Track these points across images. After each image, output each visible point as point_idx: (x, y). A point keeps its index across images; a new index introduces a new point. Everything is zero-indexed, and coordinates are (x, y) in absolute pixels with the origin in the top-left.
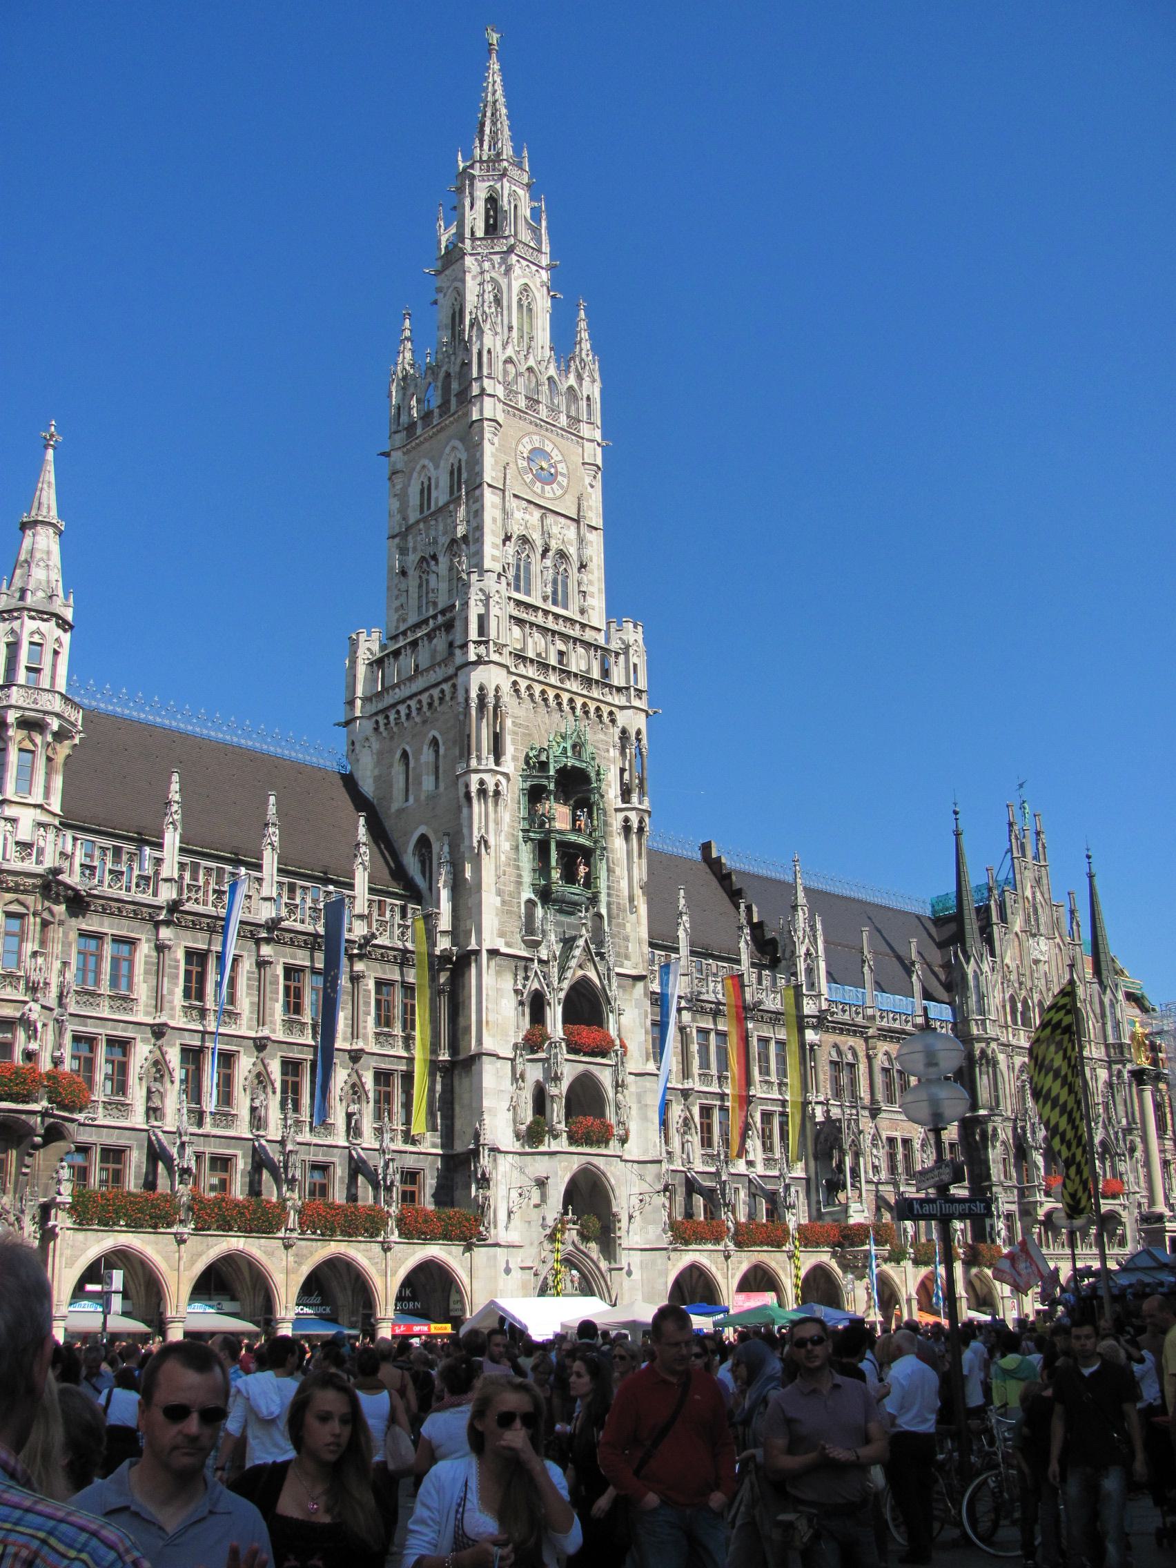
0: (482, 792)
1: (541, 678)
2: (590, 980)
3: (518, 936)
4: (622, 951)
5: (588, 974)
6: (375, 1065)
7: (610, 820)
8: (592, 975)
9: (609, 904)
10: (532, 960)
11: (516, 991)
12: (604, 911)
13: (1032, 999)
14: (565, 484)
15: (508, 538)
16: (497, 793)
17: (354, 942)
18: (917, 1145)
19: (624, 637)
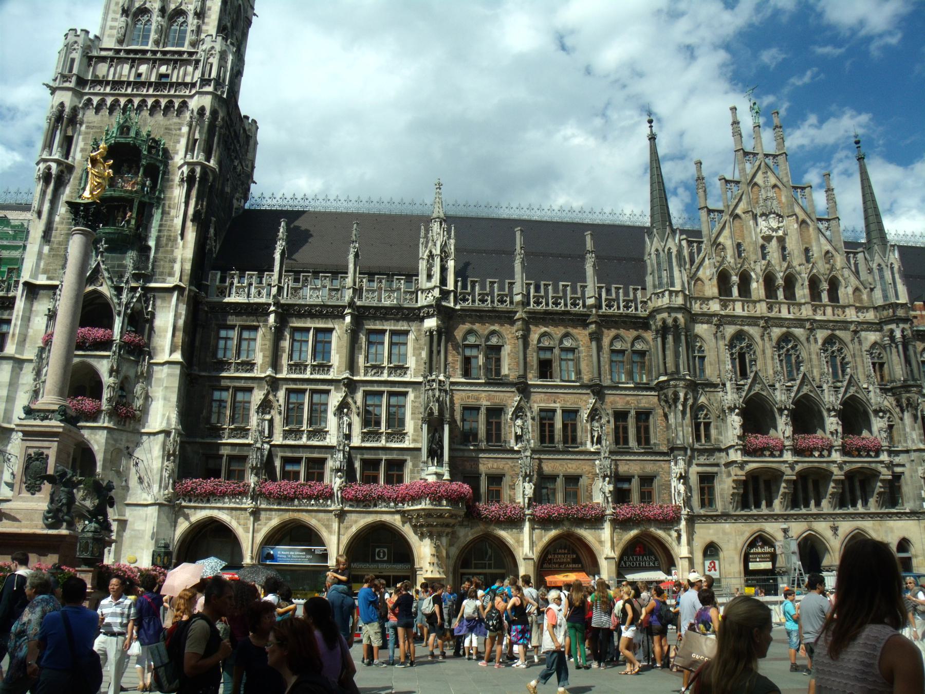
4: (167, 270)
5: (99, 288)
7: (171, 177)
9: (158, 239)
12: (152, 243)
13: (754, 270)
18: (584, 414)
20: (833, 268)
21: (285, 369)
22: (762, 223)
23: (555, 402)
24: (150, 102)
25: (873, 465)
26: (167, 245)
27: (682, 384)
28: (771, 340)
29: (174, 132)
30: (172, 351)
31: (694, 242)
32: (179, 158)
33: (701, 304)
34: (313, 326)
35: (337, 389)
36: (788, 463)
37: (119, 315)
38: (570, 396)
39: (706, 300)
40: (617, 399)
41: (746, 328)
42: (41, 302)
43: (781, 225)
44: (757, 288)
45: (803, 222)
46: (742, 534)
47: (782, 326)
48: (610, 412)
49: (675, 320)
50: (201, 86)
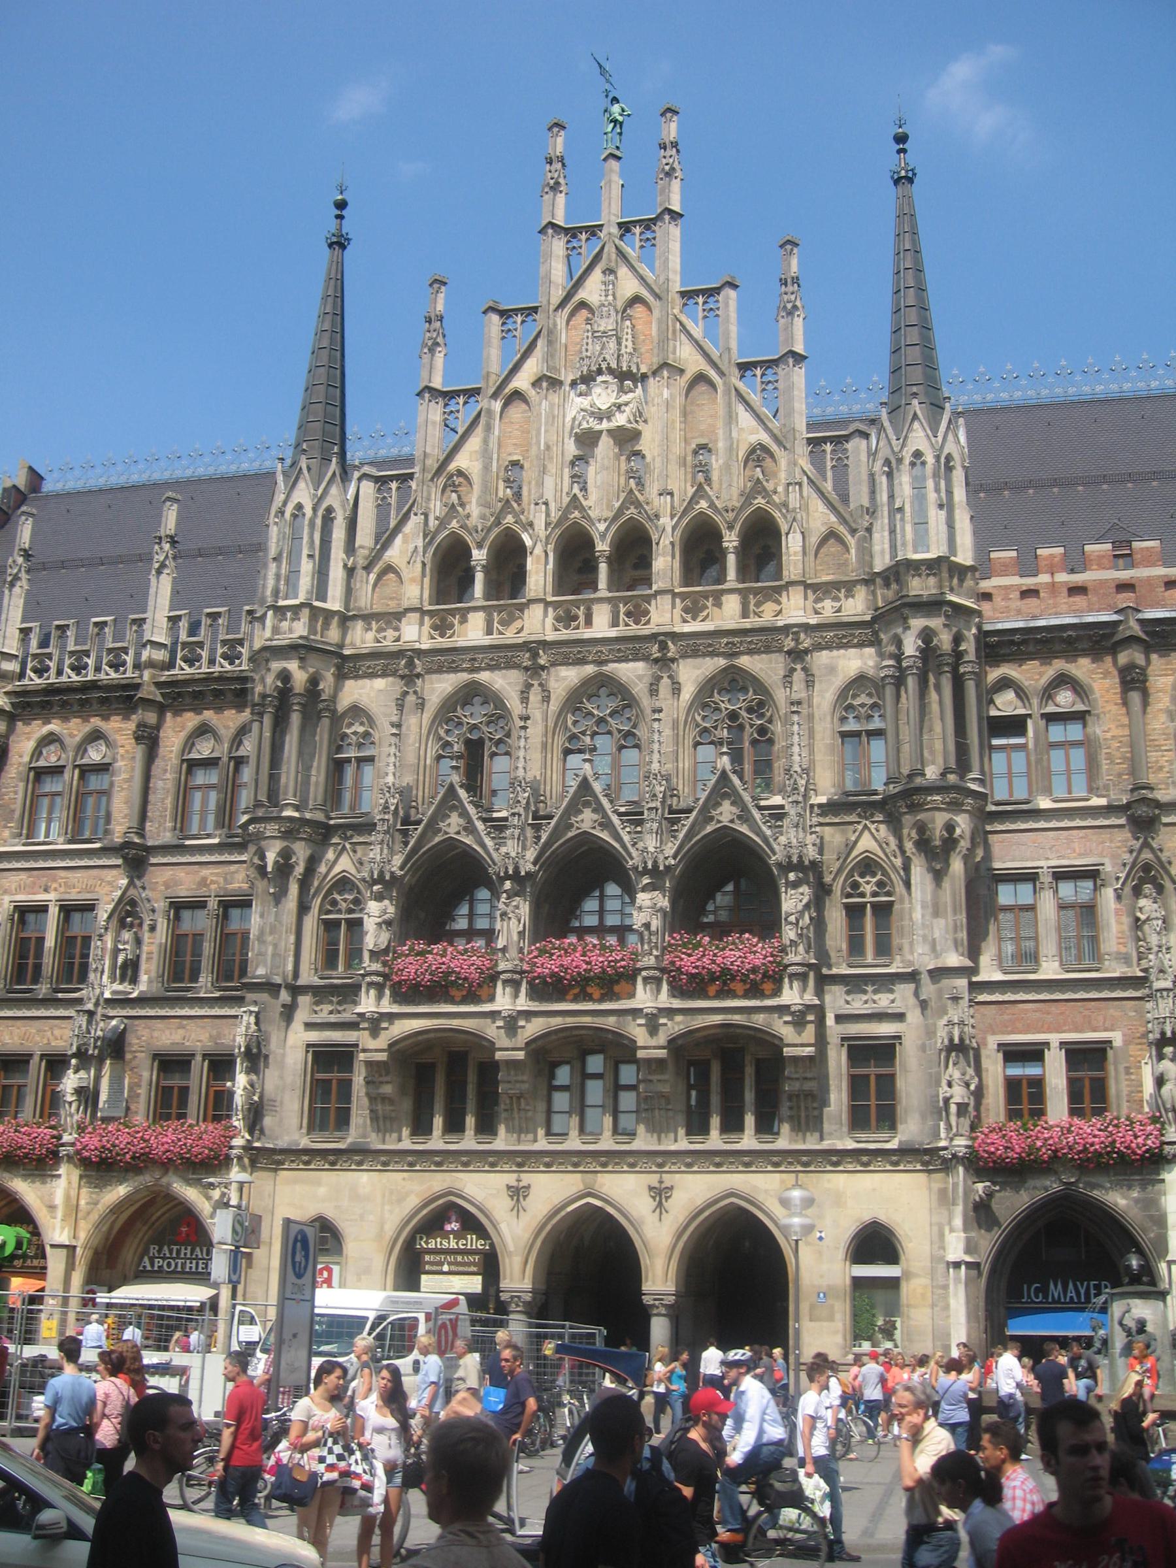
13: (531, 524)
20: (758, 488)
22: (576, 404)
23: (46, 890)
25: (759, 1020)
27: (271, 829)
28: (546, 699)
31: (392, 478)
33: (380, 630)
36: (508, 1020)
38: (79, 874)
39: (393, 618)
40: (180, 873)
41: (484, 676)
43: (625, 398)
44: (539, 573)
45: (700, 378)
46: (401, 1200)
47: (582, 662)
48: (161, 905)
49: (285, 676)
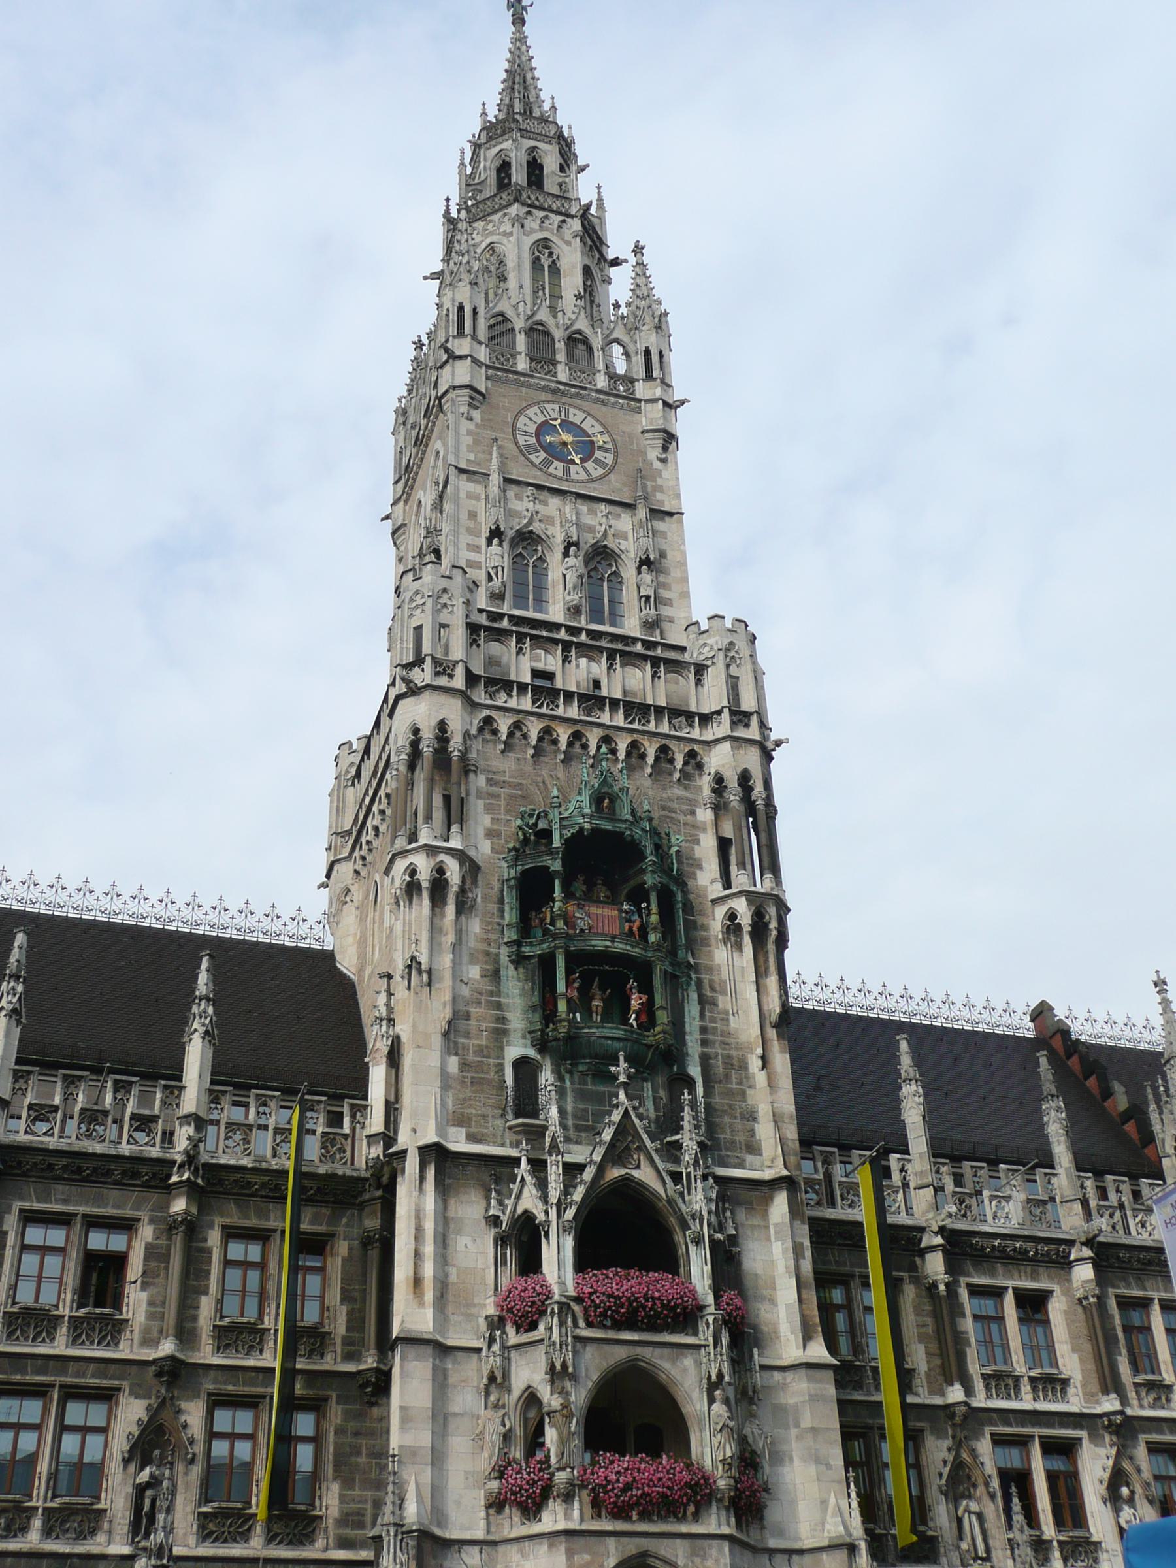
0: (412, 888)
1: (544, 710)
2: (641, 1185)
3: (499, 1122)
4: (741, 1138)
5: (636, 1173)
6: (211, 1387)
7: (701, 920)
8: (644, 1174)
9: (705, 1060)
10: (516, 1161)
11: (495, 1221)
12: (695, 1071)
14: (609, 459)
15: (496, 533)
16: (439, 885)
17: (174, 1162)
19: (711, 641)
21: (979, 1385)
24: (622, 747)
26: (727, 1077)
29: (681, 818)
30: (807, 1337)
32: (707, 879)
34: (1010, 1283)
35: (1095, 1438)
37: (698, 1241)
42: (464, 1198)
50: (734, 724)
